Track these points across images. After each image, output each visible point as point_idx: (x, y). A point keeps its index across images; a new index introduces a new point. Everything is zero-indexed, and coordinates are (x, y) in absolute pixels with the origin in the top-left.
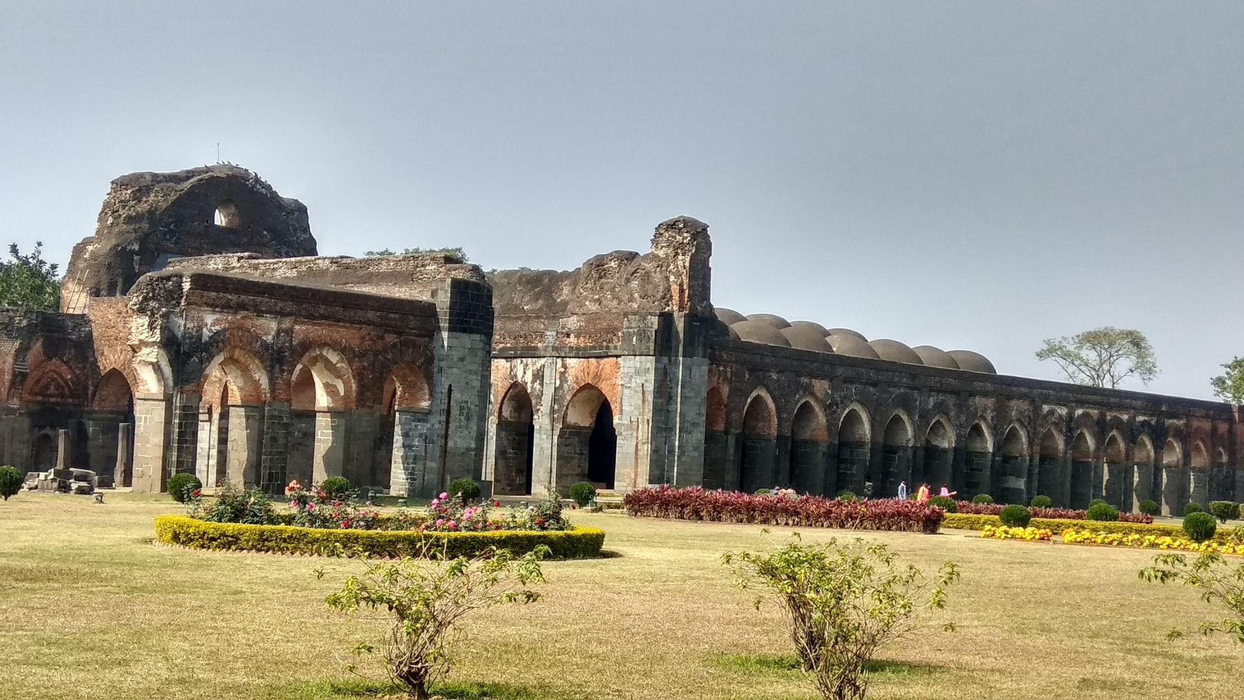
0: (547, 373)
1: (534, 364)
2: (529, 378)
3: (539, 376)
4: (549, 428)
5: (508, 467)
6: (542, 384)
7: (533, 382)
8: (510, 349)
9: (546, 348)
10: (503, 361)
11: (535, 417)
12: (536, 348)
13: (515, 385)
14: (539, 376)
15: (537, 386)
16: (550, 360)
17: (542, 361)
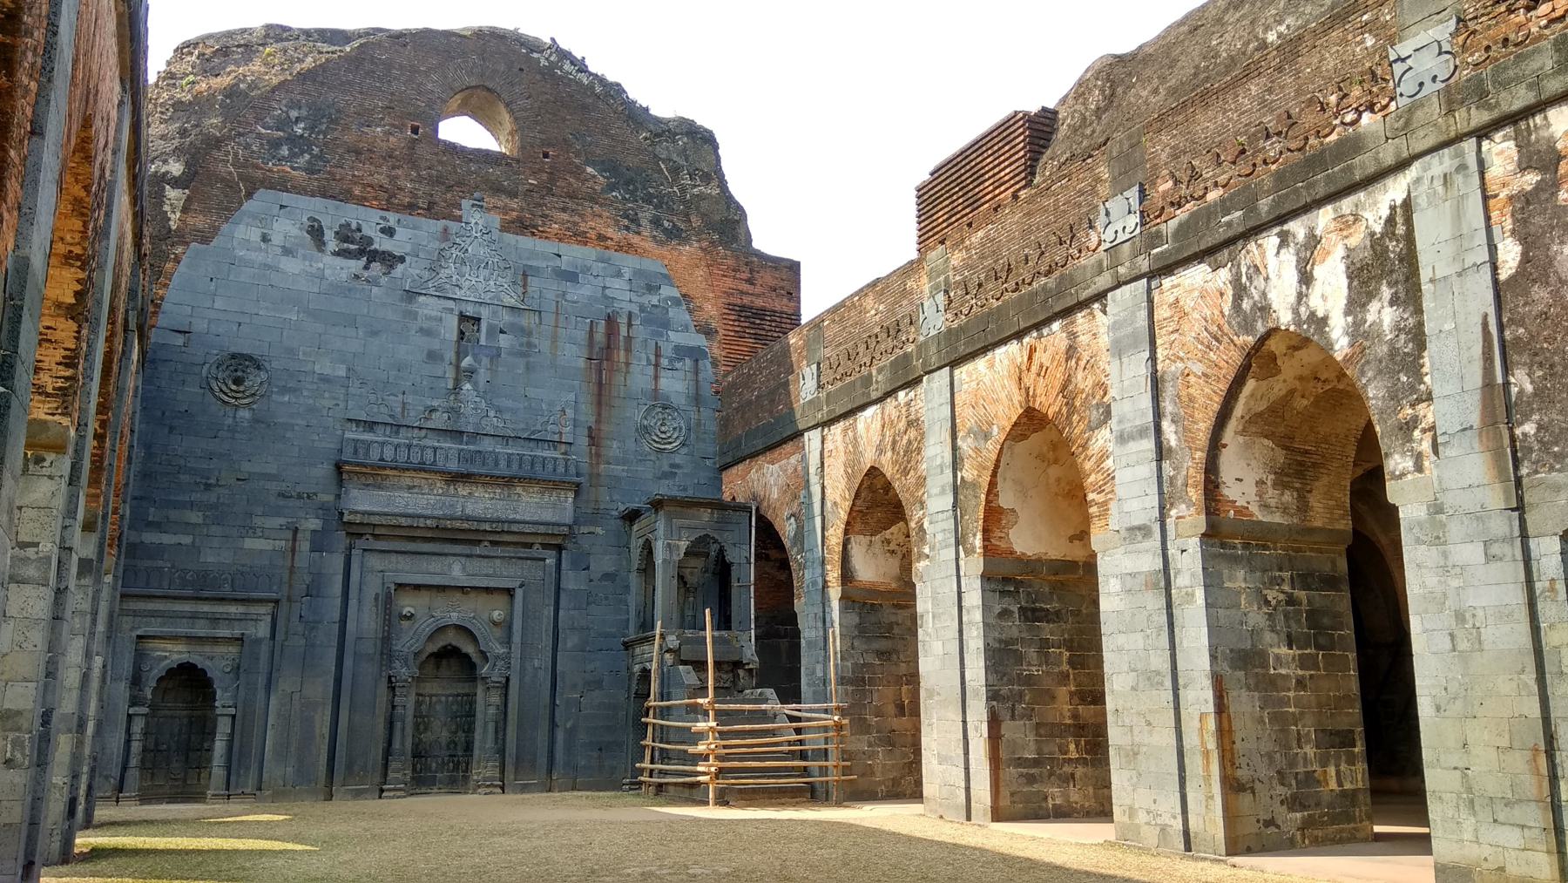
0: (1430, 232)
1: (1340, 231)
2: (1331, 289)
3: (1389, 265)
4: (1495, 498)
5: (1280, 719)
6: (1410, 296)
7: (1357, 304)
8: (1225, 206)
9: (1406, 125)
10: (1196, 276)
11: (1397, 463)
12: (1353, 145)
13: (1258, 360)
14: (1389, 265)
15: (1383, 314)
16: (1441, 163)
17: (1395, 190)
